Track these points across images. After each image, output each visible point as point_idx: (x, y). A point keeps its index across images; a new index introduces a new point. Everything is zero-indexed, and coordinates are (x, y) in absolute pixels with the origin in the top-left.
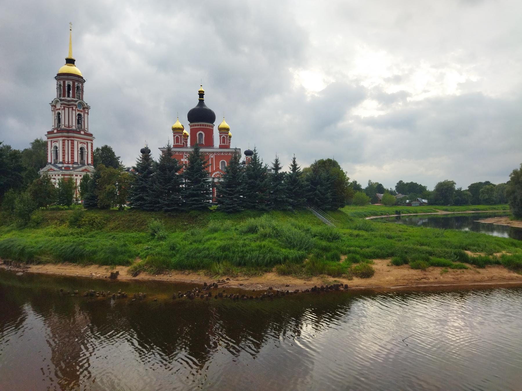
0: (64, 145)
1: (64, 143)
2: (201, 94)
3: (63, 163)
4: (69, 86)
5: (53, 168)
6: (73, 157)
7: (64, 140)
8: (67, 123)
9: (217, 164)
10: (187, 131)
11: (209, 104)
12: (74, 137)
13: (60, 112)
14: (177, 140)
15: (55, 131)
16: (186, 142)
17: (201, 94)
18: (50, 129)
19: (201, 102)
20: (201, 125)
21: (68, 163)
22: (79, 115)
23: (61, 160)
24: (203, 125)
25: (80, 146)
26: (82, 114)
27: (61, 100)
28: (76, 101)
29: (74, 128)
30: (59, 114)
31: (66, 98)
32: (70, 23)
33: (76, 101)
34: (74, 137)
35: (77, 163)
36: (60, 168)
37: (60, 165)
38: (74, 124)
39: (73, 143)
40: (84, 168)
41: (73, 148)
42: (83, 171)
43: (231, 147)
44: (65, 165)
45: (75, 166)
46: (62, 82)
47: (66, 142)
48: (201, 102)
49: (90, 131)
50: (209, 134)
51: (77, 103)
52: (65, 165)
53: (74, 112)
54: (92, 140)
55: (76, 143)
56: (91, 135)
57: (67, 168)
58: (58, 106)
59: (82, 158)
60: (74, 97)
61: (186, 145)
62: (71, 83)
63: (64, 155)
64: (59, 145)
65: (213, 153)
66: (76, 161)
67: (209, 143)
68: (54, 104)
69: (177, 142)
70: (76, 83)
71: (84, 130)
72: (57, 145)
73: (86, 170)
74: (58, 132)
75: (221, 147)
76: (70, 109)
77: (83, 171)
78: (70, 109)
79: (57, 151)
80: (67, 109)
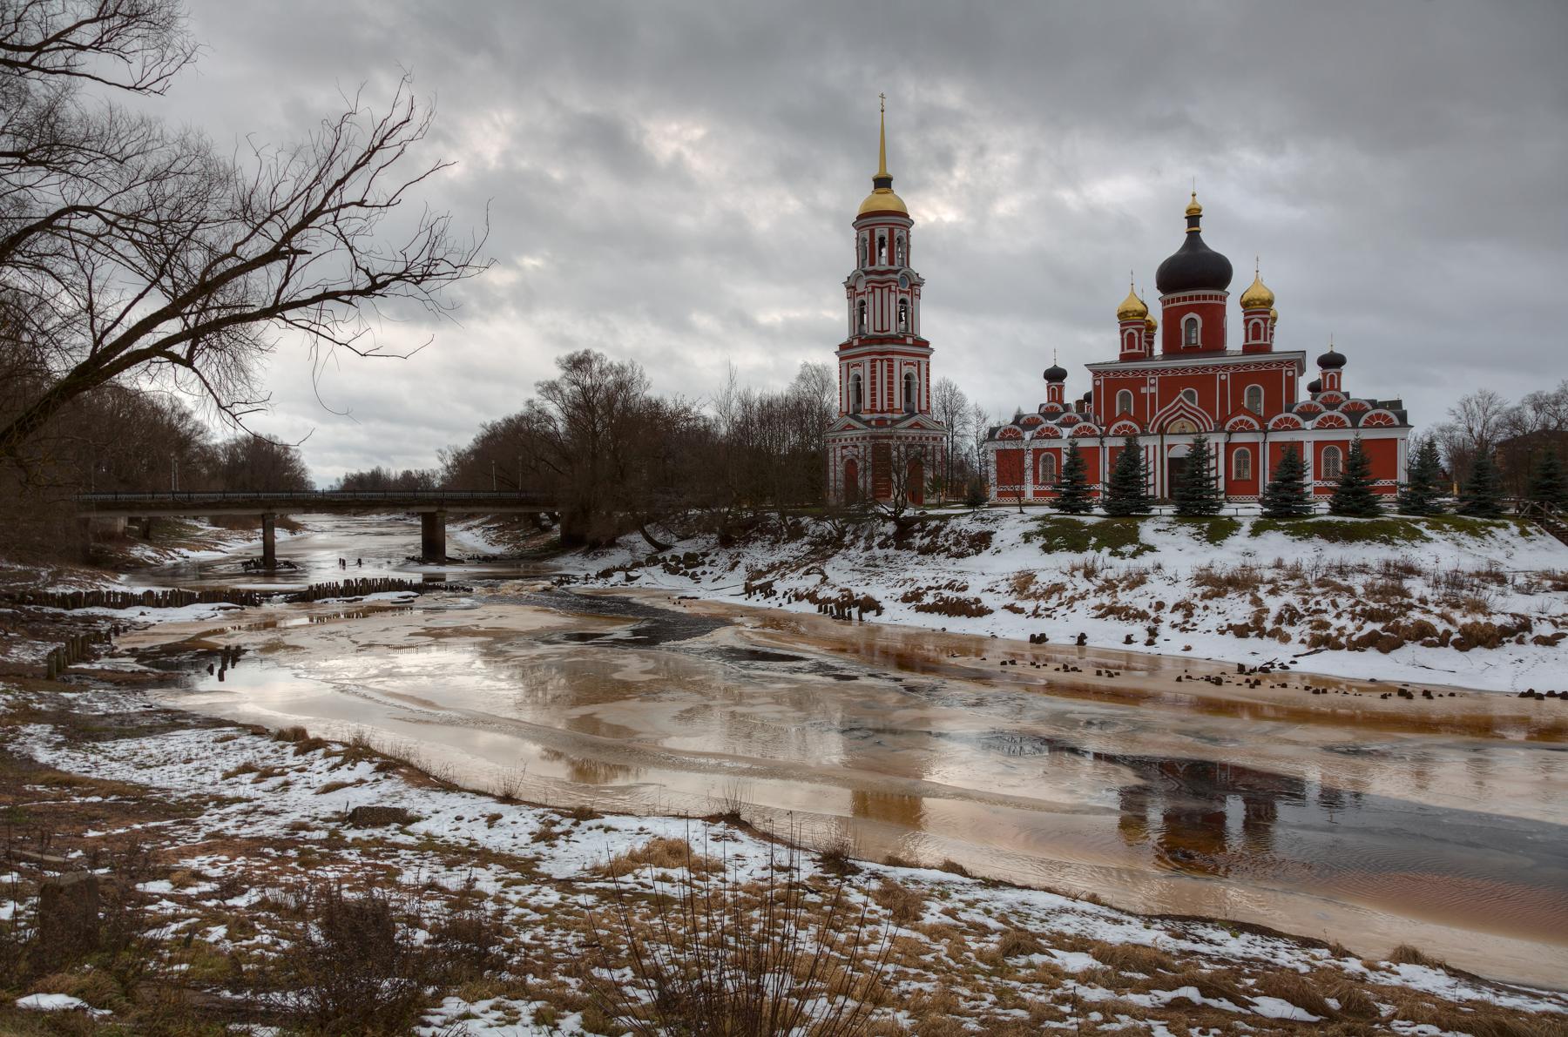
0: (873, 372)
1: (873, 366)
2: (1193, 218)
3: (872, 411)
4: (882, 239)
5: (853, 422)
6: (891, 400)
7: (873, 361)
9: (1237, 397)
10: (1156, 314)
11: (1213, 240)
12: (893, 353)
13: (864, 298)
14: (1128, 341)
15: (856, 342)
16: (1151, 344)
17: (1193, 218)
18: (844, 339)
19: (1193, 237)
20: (1191, 298)
21: (882, 411)
22: (903, 301)
23: (868, 406)
24: (1198, 298)
25: (905, 370)
26: (908, 298)
27: (867, 273)
28: (896, 272)
29: (893, 332)
30: (863, 303)
31: (877, 267)
32: (882, 96)
33: (896, 272)
34: (893, 353)
36: (867, 423)
37: (867, 417)
39: (891, 366)
40: (912, 420)
41: (891, 377)
42: (911, 427)
43: (1275, 348)
44: (876, 416)
45: (896, 416)
46: (867, 234)
48: (1193, 237)
49: (924, 335)
50: (1214, 319)
51: (898, 277)
52: (876, 416)
53: (893, 296)
54: (927, 357)
55: (896, 365)
56: (925, 344)
57: (881, 423)
58: (860, 288)
59: (908, 399)
60: (891, 262)
61: (1151, 351)
62: (885, 232)
63: (873, 395)
64: (864, 371)
65: (1226, 367)
66: (897, 405)
67: (1214, 341)
68: (852, 283)
69: (1131, 346)
70: (897, 232)
71: (913, 335)
72: (859, 371)
73: (917, 424)
74: (863, 343)
75: (1247, 350)
76: (886, 291)
77: (911, 427)
78: (886, 291)
79: (858, 386)
80: (878, 291)
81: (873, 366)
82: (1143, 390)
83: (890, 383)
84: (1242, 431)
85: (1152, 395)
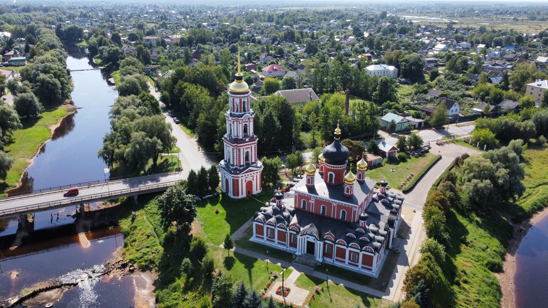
1: (233, 151)
3: (233, 165)
6: (240, 162)
8: (236, 134)
25: (245, 151)
26: (248, 123)
35: (243, 166)
38: (241, 134)
39: (239, 151)
44: (234, 167)
47: (235, 150)
55: (242, 150)
63: (233, 160)
66: (242, 164)
80: (235, 123)
81: (233, 151)
82: (310, 201)
83: (240, 157)
84: (329, 240)
85: (313, 204)
